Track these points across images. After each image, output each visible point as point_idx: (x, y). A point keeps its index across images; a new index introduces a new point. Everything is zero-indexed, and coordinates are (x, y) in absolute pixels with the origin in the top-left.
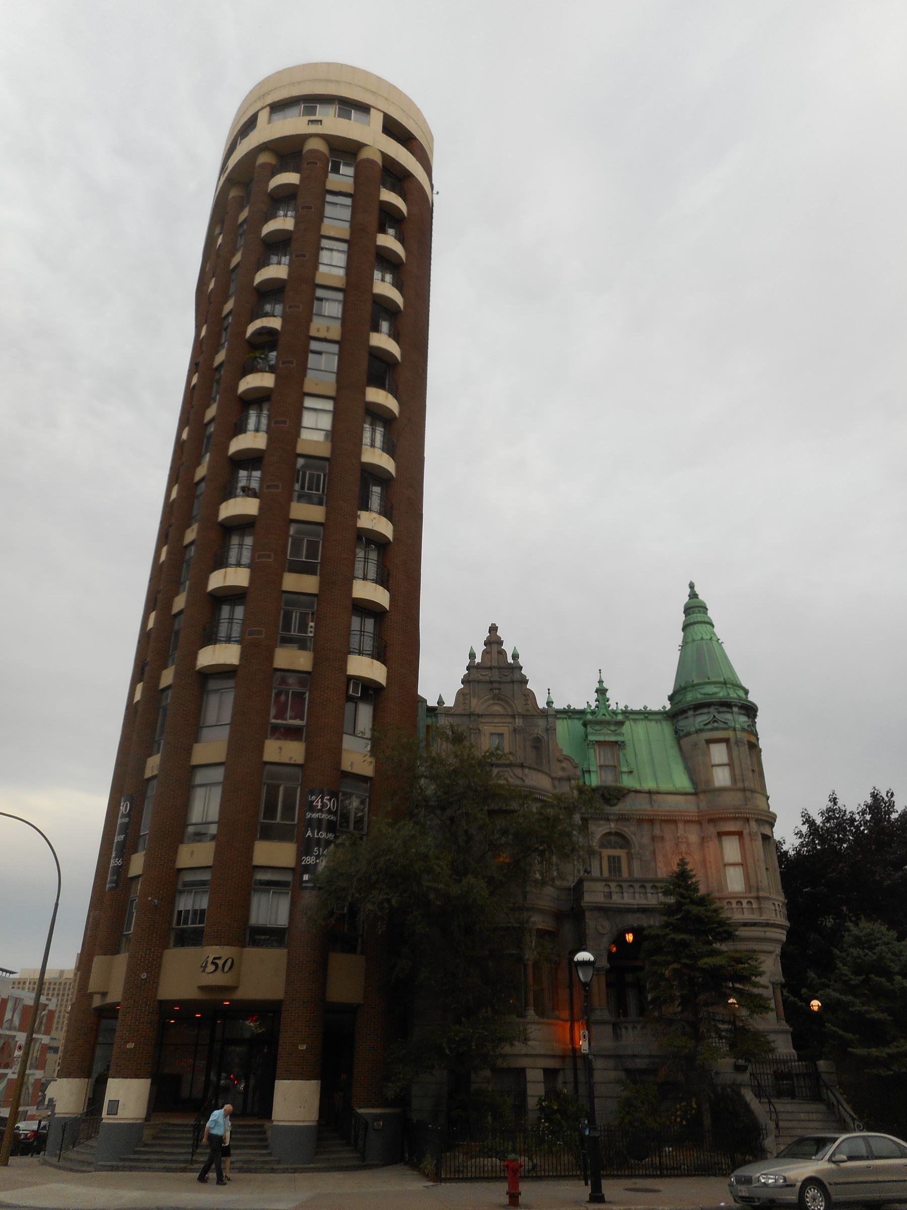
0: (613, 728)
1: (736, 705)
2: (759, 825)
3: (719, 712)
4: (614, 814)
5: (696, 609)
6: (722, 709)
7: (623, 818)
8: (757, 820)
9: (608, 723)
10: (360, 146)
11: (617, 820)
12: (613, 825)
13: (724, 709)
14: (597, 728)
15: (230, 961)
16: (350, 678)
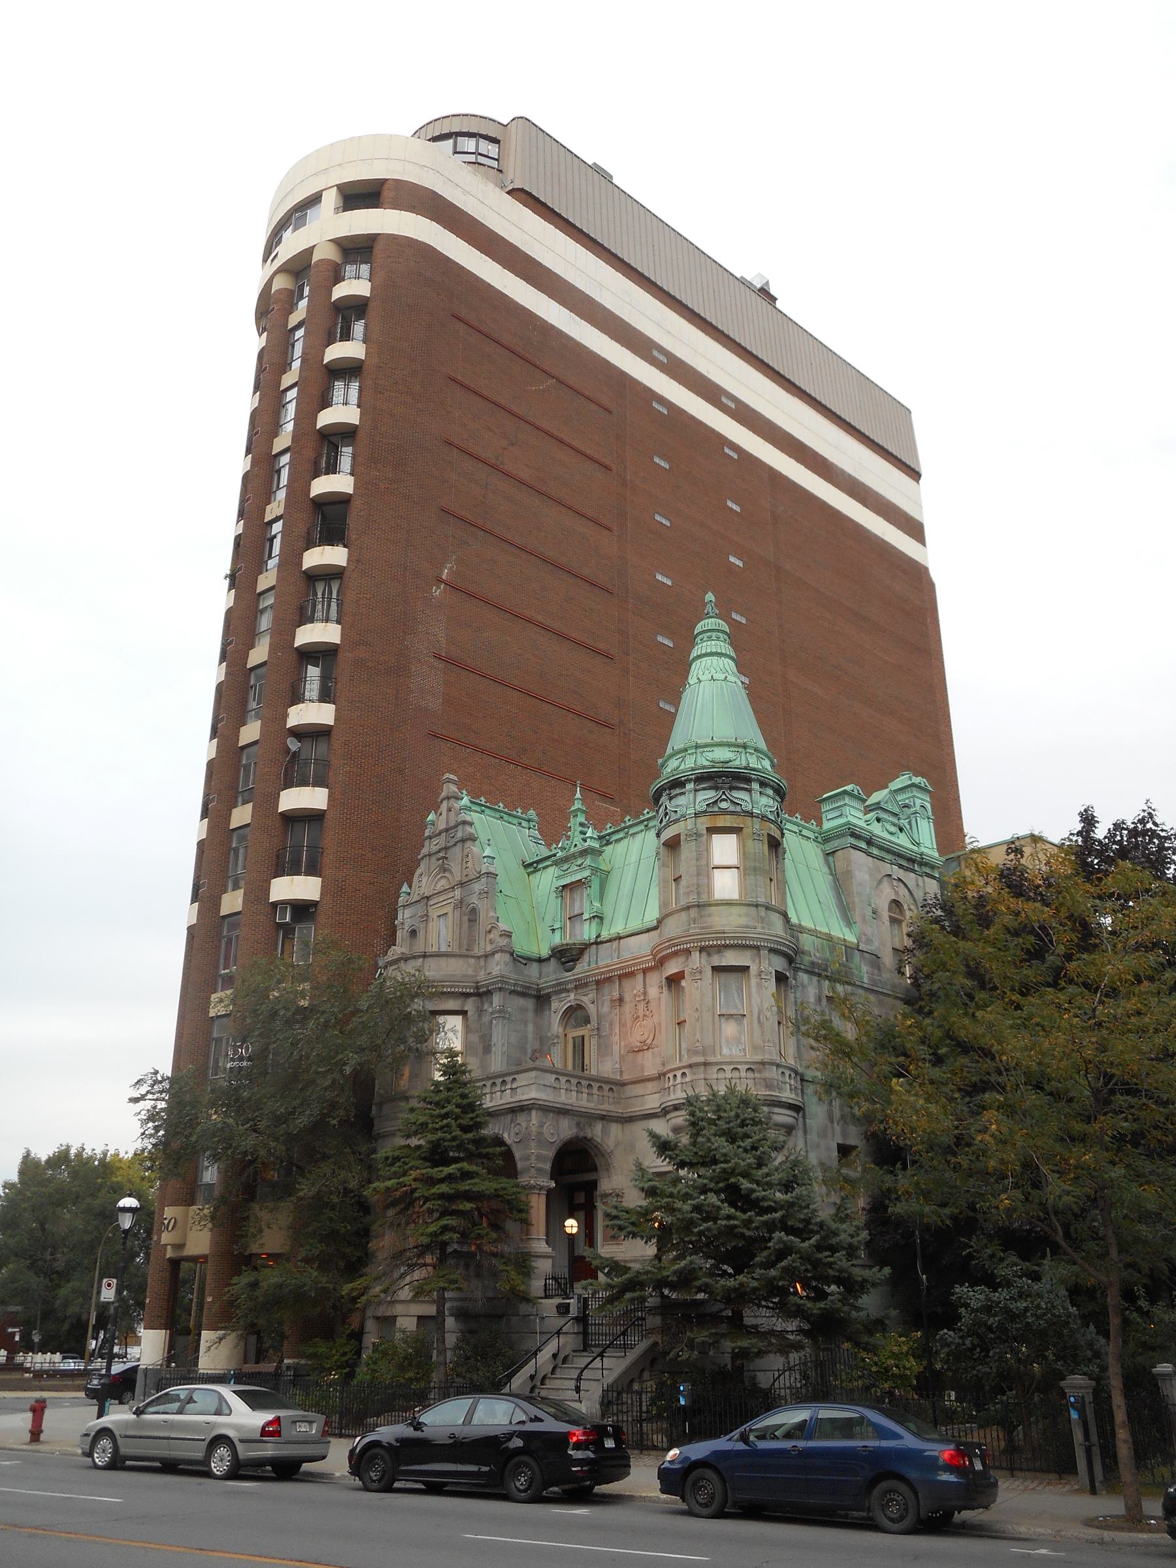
0: (579, 861)
1: (689, 781)
2: (709, 955)
3: (671, 799)
4: (570, 981)
5: (705, 635)
6: (674, 792)
7: (581, 985)
8: (702, 949)
9: (574, 856)
10: (310, 251)
11: (576, 987)
12: (572, 996)
13: (678, 791)
14: (566, 866)
15: (173, 1220)
16: (275, 905)
